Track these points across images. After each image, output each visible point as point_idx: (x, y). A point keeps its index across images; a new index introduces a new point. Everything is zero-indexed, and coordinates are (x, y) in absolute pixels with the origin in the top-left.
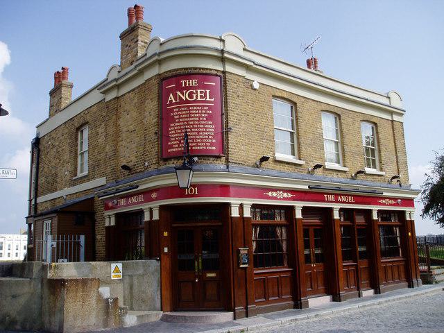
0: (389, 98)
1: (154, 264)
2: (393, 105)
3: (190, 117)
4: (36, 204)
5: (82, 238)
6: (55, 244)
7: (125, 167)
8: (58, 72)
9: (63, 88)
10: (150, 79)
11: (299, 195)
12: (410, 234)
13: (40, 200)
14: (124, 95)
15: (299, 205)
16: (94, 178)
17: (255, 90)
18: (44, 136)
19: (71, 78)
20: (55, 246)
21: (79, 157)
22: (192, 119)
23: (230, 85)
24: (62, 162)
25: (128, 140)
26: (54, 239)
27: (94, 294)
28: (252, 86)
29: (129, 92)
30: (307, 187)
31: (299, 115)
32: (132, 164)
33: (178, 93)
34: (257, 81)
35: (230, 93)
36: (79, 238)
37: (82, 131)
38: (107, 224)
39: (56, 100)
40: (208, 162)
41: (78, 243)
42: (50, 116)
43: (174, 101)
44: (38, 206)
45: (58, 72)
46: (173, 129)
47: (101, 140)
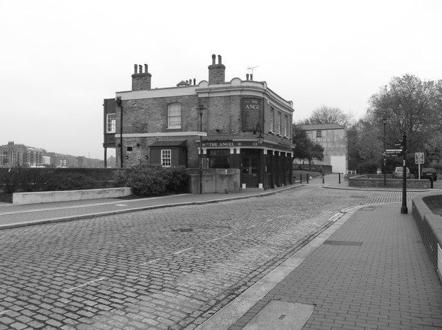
7: (218, 131)
11: (275, 146)
13: (124, 135)
42: (133, 90)
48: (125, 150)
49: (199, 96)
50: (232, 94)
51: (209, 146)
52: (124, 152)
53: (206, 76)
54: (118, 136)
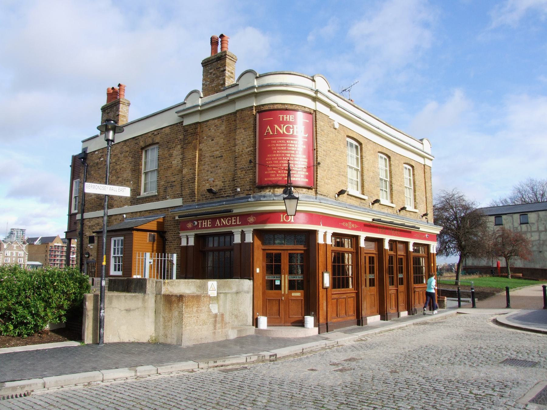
0: (422, 144)
1: (247, 284)
2: (425, 150)
3: (287, 150)
4: (83, 220)
5: (175, 255)
6: (152, 261)
7: (210, 191)
8: (113, 88)
9: (121, 106)
10: (242, 110)
12: (432, 265)
13: (87, 215)
14: (207, 121)
15: (363, 235)
16: (165, 198)
17: (335, 129)
18: (95, 151)
19: (126, 96)
20: (152, 263)
21: (143, 176)
22: (288, 152)
23: (320, 123)
24: (120, 179)
25: (213, 165)
26: (151, 257)
27: (204, 309)
28: (333, 125)
29: (214, 119)
30: (371, 220)
31: (364, 154)
32: (218, 187)
33: (276, 126)
34: (338, 120)
35: (319, 130)
36: (172, 257)
37: (146, 151)
38: (184, 243)
39: (111, 115)
40: (302, 192)
41: (171, 262)
43: (271, 133)
44: (85, 222)
45: (113, 88)
46: (270, 159)
47: (176, 162)
48: (86, 240)
49: (187, 122)
50: (240, 106)
51: (197, 227)
52: (85, 245)
53: (196, 81)
54: (79, 217)
